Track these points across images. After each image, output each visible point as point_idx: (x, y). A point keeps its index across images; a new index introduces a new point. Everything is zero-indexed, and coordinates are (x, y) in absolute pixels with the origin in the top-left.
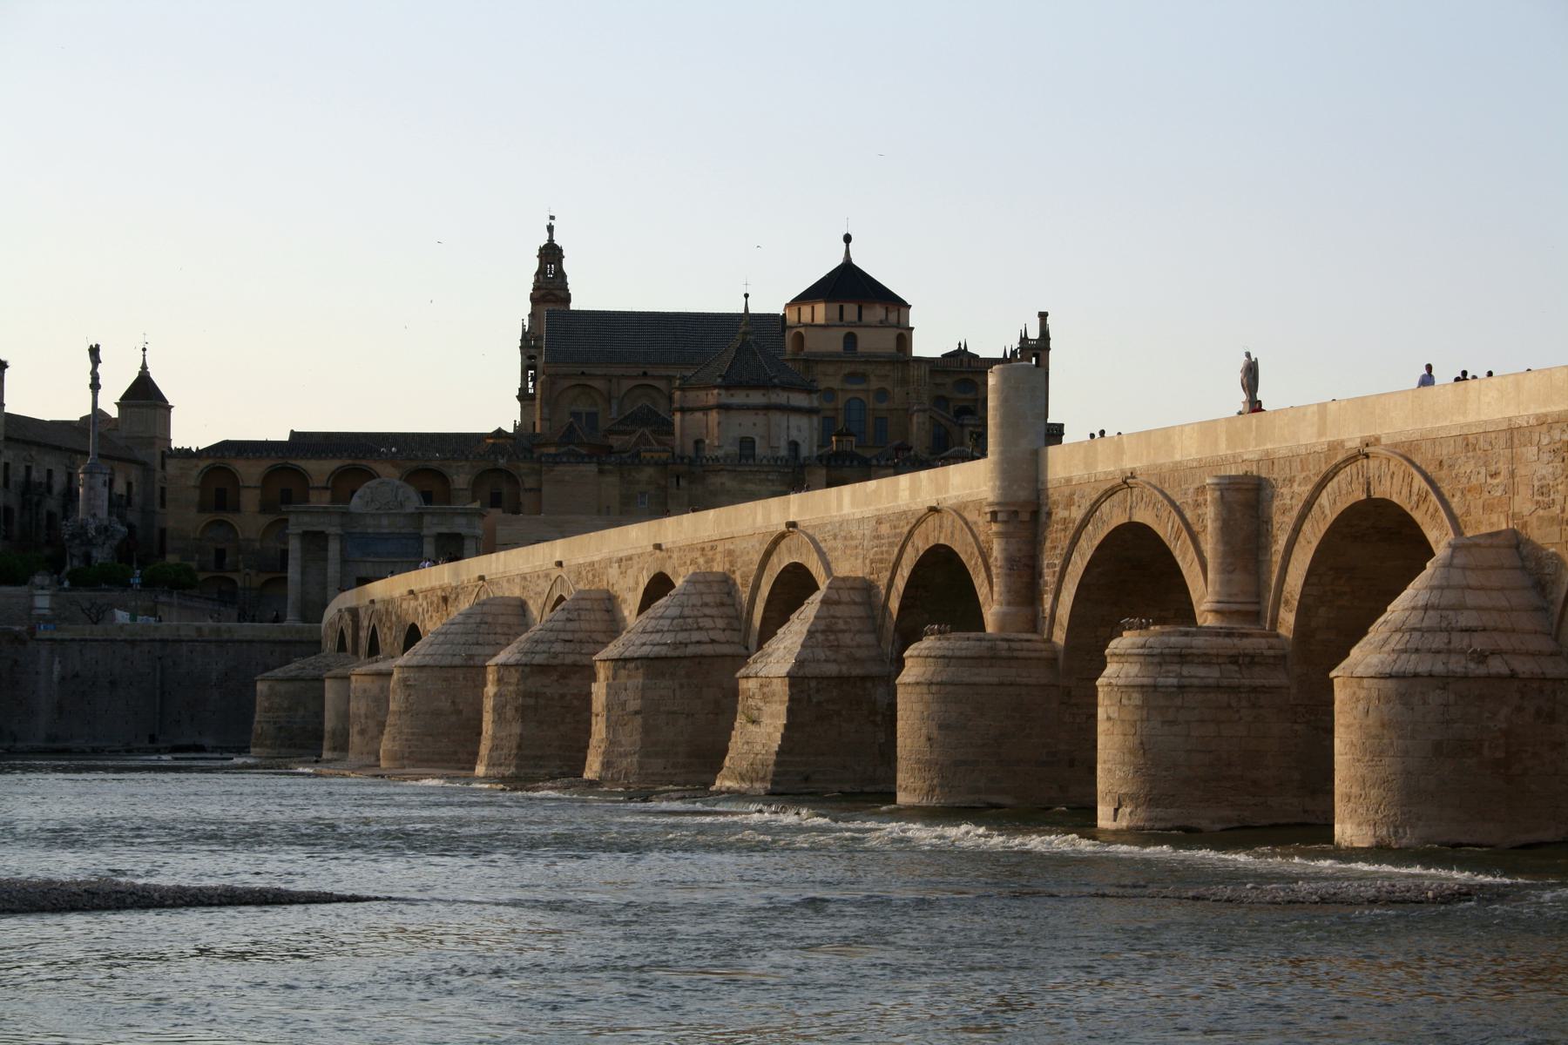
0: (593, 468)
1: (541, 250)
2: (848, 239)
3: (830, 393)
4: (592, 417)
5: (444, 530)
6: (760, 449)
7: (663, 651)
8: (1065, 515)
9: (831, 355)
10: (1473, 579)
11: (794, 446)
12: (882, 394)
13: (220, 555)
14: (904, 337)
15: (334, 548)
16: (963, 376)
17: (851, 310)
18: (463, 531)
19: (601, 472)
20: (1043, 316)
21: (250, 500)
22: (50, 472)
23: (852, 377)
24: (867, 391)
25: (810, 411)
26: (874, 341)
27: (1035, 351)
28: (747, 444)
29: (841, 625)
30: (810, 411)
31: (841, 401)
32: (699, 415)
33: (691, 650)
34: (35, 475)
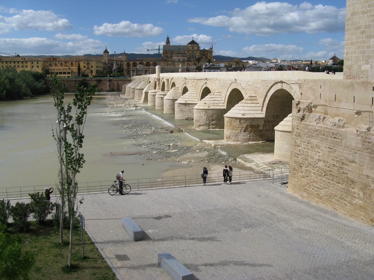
0: (164, 62)
2: (193, 38)
3: (190, 53)
4: (168, 56)
6: (181, 60)
7: (140, 88)
8: (161, 80)
10: (174, 90)
11: (184, 60)
12: (195, 54)
13: (129, 71)
14: (199, 47)
15: (135, 71)
17: (193, 45)
20: (212, 46)
21: (131, 65)
23: (192, 52)
25: (186, 56)
27: (212, 49)
29: (150, 87)
30: (186, 56)
32: (175, 57)
33: (142, 88)
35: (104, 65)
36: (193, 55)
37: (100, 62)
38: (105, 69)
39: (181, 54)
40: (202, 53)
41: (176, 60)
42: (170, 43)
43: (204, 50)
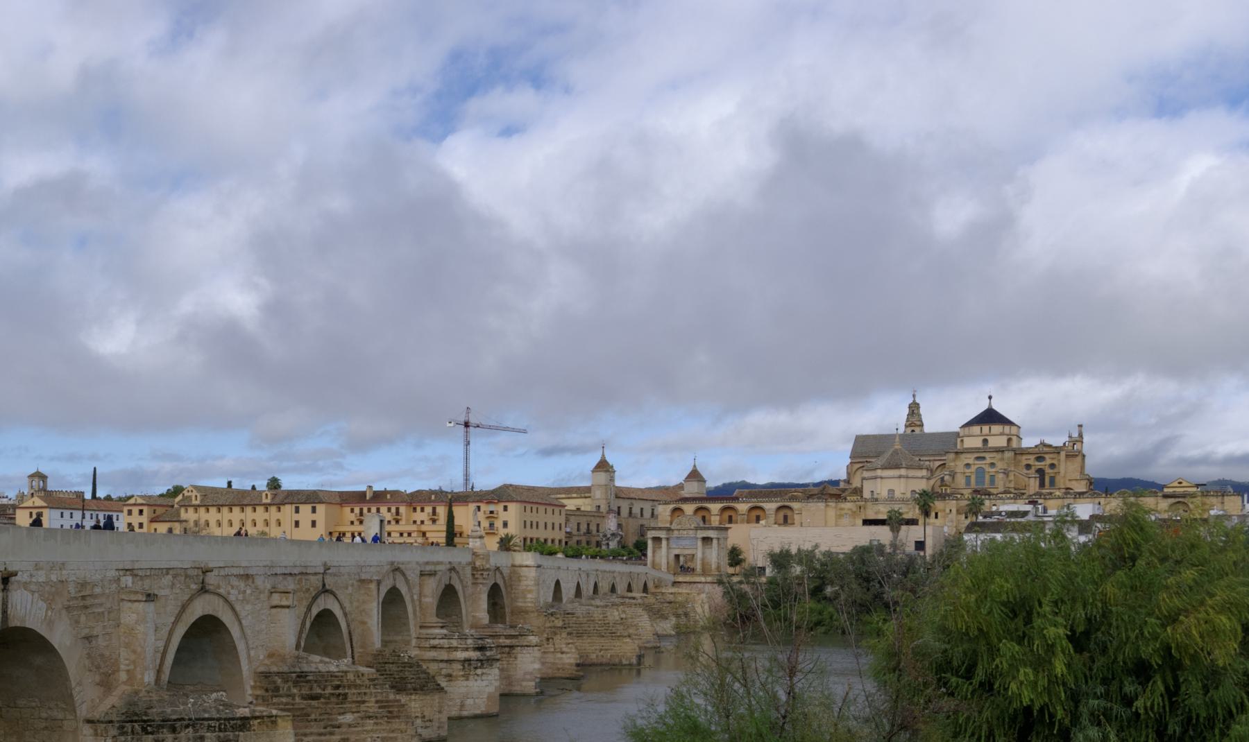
0: (824, 504)
1: (910, 405)
3: (968, 465)
5: (705, 536)
6: (897, 494)
9: (976, 448)
12: (992, 465)
15: (664, 543)
16: (1039, 455)
17: (986, 429)
18: (712, 536)
19: (827, 506)
22: (642, 509)
23: (978, 458)
24: (986, 464)
25: (922, 478)
26: (995, 442)
28: (891, 491)
30: (922, 478)
31: (973, 469)
34: (634, 511)
35: (589, 519)
36: (981, 471)
37: (550, 509)
38: (594, 532)
39: (897, 467)
40: (1031, 462)
41: (875, 496)
42: (922, 425)
43: (1042, 451)
